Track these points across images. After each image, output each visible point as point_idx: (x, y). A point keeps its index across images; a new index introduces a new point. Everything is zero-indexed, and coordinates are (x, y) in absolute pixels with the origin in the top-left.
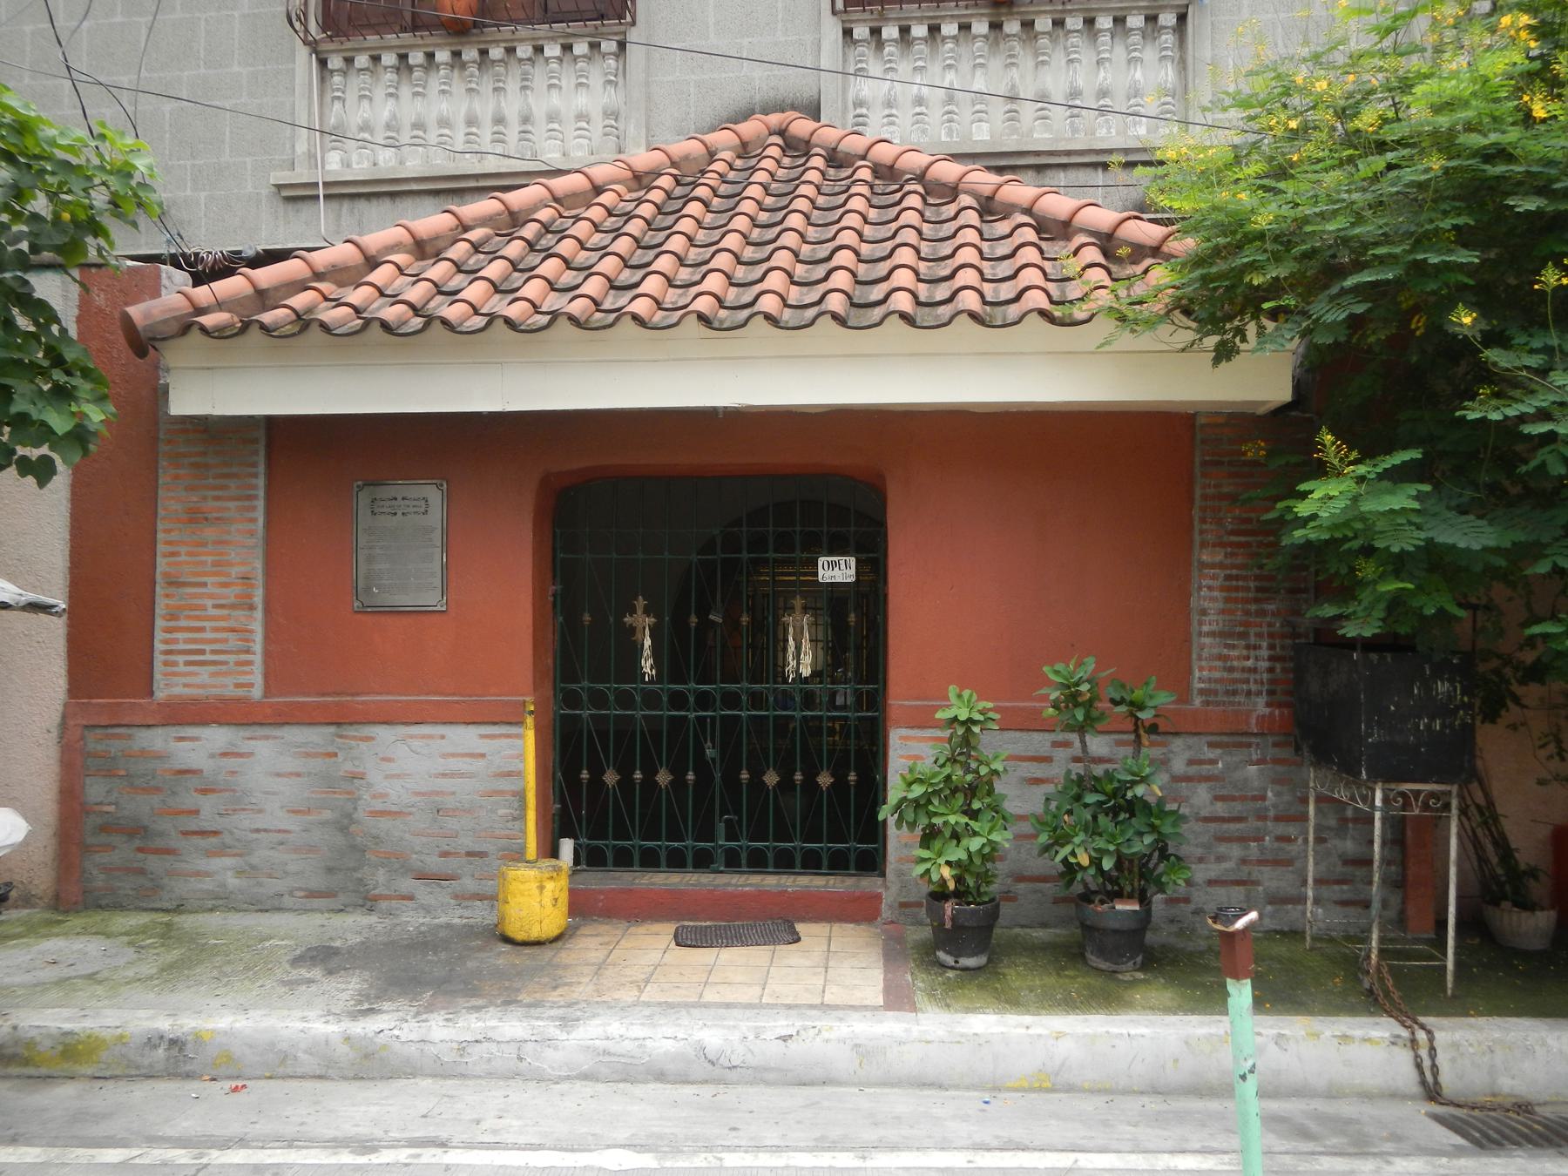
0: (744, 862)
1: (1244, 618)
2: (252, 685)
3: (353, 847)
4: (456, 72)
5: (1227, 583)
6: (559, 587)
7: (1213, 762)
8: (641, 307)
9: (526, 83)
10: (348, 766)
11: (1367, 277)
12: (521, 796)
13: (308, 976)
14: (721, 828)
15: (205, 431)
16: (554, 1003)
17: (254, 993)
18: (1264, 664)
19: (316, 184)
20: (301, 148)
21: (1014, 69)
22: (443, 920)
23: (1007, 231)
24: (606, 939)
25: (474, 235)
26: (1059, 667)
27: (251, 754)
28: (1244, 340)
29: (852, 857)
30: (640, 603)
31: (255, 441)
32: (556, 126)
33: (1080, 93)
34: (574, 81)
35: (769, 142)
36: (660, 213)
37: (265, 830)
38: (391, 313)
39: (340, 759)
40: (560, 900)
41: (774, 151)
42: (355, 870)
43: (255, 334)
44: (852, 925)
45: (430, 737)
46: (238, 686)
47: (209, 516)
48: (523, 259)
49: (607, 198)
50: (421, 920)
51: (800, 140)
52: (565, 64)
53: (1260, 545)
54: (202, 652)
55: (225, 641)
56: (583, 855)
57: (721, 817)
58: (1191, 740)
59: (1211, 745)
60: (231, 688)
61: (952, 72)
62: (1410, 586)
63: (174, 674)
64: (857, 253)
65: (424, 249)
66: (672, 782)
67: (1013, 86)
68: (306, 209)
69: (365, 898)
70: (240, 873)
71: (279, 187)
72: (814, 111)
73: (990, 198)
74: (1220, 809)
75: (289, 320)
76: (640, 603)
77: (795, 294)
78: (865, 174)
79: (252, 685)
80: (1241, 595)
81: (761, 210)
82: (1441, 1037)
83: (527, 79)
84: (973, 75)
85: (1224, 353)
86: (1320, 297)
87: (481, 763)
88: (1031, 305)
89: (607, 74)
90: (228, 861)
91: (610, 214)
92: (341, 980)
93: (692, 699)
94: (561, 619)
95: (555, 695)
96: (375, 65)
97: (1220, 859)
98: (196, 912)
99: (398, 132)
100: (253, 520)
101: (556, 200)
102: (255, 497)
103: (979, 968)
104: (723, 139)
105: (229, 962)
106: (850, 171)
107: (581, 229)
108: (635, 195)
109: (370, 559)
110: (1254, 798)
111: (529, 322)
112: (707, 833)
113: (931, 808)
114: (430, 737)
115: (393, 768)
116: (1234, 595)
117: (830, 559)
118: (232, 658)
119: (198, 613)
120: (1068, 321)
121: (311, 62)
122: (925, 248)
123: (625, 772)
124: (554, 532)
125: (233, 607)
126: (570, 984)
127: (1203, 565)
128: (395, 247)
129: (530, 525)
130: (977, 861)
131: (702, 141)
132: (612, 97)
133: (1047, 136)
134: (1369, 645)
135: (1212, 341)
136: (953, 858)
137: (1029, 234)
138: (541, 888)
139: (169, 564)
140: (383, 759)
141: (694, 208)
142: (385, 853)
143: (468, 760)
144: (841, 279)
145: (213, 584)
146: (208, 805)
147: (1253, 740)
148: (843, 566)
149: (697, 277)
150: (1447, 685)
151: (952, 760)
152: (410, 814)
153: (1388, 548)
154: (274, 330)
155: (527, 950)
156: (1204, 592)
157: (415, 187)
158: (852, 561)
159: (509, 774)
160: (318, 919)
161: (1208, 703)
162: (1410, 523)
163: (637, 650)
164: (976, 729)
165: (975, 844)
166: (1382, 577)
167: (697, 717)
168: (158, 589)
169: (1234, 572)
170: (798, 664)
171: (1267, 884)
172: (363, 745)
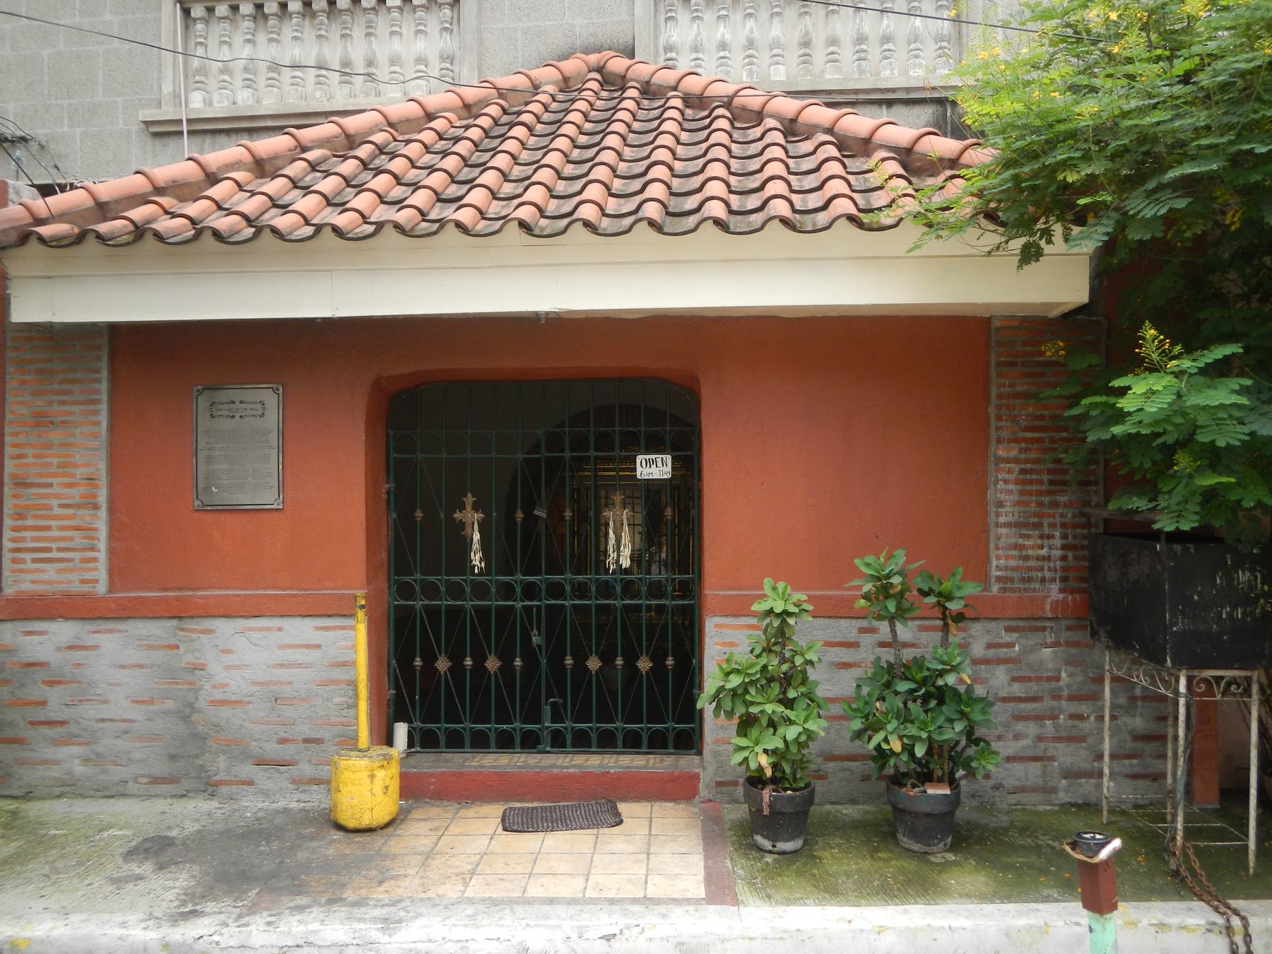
0: (568, 742)
1: (1038, 509)
2: (96, 581)
3: (195, 736)
4: (307, 21)
5: (1021, 477)
6: (393, 485)
7: (1011, 645)
8: (465, 216)
9: (371, 30)
10: (190, 658)
11: (1189, 169)
12: (353, 684)
13: (138, 871)
14: (547, 710)
15: (50, 338)
16: (378, 900)
17: (80, 893)
18: (1057, 553)
19: (180, 121)
20: (167, 88)
21: (807, 18)
22: (281, 804)
23: (811, 149)
24: (436, 823)
25: (311, 155)
26: (870, 559)
27: (96, 647)
28: (1049, 242)
29: (671, 737)
30: (469, 499)
31: (99, 348)
32: (397, 69)
33: (866, 39)
34: (413, 29)
35: (589, 77)
36: (487, 137)
37: (110, 720)
38: (223, 223)
39: (181, 651)
40: (390, 789)
41: (594, 85)
42: (197, 756)
43: (91, 244)
44: (671, 805)
45: (268, 629)
46: (83, 582)
48: (356, 176)
49: (438, 124)
50: (260, 805)
51: (616, 75)
52: (405, 14)
53: (1053, 441)
54: (49, 550)
55: (71, 539)
56: (417, 738)
57: (547, 700)
58: (992, 625)
59: (1008, 629)
60: (77, 584)
61: (752, 20)
62: (1233, 480)
63: (22, 571)
64: (671, 168)
65: (262, 168)
66: (500, 668)
67: (807, 33)
68: (172, 143)
69: (207, 784)
70: (86, 761)
71: (147, 123)
72: (631, 54)
73: (793, 121)
74: (1017, 690)
75: (126, 230)
76: (469, 499)
77: (612, 205)
78: (677, 103)
79: (96, 581)
80: (1034, 488)
81: (581, 133)
82: (1255, 924)
83: (370, 27)
84: (771, 23)
85: (1030, 255)
86: (1135, 193)
87: (317, 654)
88: (840, 211)
89: (442, 22)
90: (75, 750)
91: (441, 138)
92: (169, 876)
93: (518, 590)
94: (394, 515)
95: (389, 587)
96: (234, 14)
97: (1017, 737)
98: (45, 798)
99: (255, 74)
101: (391, 125)
103: (796, 851)
104: (547, 75)
105: (63, 856)
106: (662, 102)
107: (413, 150)
108: (464, 122)
109: (209, 460)
110: (1049, 679)
111: (357, 230)
112: (533, 715)
113: (748, 697)
114: (268, 629)
115: (232, 659)
116: (1028, 488)
117: (647, 457)
118: (77, 556)
119: (44, 512)
120: (876, 226)
121: (175, 14)
122: (735, 165)
123: (456, 658)
124: (388, 435)
125: (78, 506)
126: (395, 878)
127: (999, 460)
128: (236, 165)
129: (362, 427)
130: (794, 749)
131: (527, 76)
132: (447, 43)
133: (837, 76)
134: (1177, 537)
135: (1017, 244)
136: (770, 747)
137: (832, 151)
138: (372, 777)
139: (14, 465)
140: (224, 651)
141: (519, 131)
142: (225, 740)
143: (305, 651)
144: (656, 190)
145: (59, 485)
146: (55, 696)
147: (1048, 624)
148: (660, 464)
149: (520, 190)
150: (1248, 574)
151: (768, 650)
152: (250, 703)
153: (1213, 442)
154: (110, 240)
155: (358, 838)
156: (1001, 486)
157: (270, 123)
158: (668, 458)
159: (343, 664)
160: (161, 805)
161: (1004, 590)
162: (1231, 416)
163: (466, 544)
164: (791, 621)
165: (792, 733)
166: (1199, 471)
167: (523, 606)
168: (6, 490)
169: (1028, 466)
170: (619, 556)
171: (1062, 759)
172: (204, 638)
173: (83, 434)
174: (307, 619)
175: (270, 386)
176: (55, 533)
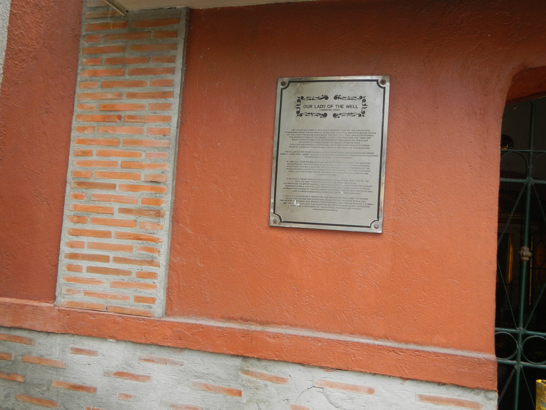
2: (153, 300)
15: (125, 25)
27: (147, 378)
31: (175, 34)
39: (244, 399)
45: (355, 388)
46: (139, 299)
47: (122, 114)
54: (105, 259)
55: (130, 249)
60: (132, 301)
63: (76, 280)
79: (153, 300)
100: (167, 119)
102: (170, 94)
109: (292, 166)
114: (355, 388)
118: (134, 268)
119: (104, 217)
125: (140, 212)
139: (78, 163)
168: (68, 188)
173: (150, 130)
174: (408, 383)
175: (374, 78)
176: (113, 241)
